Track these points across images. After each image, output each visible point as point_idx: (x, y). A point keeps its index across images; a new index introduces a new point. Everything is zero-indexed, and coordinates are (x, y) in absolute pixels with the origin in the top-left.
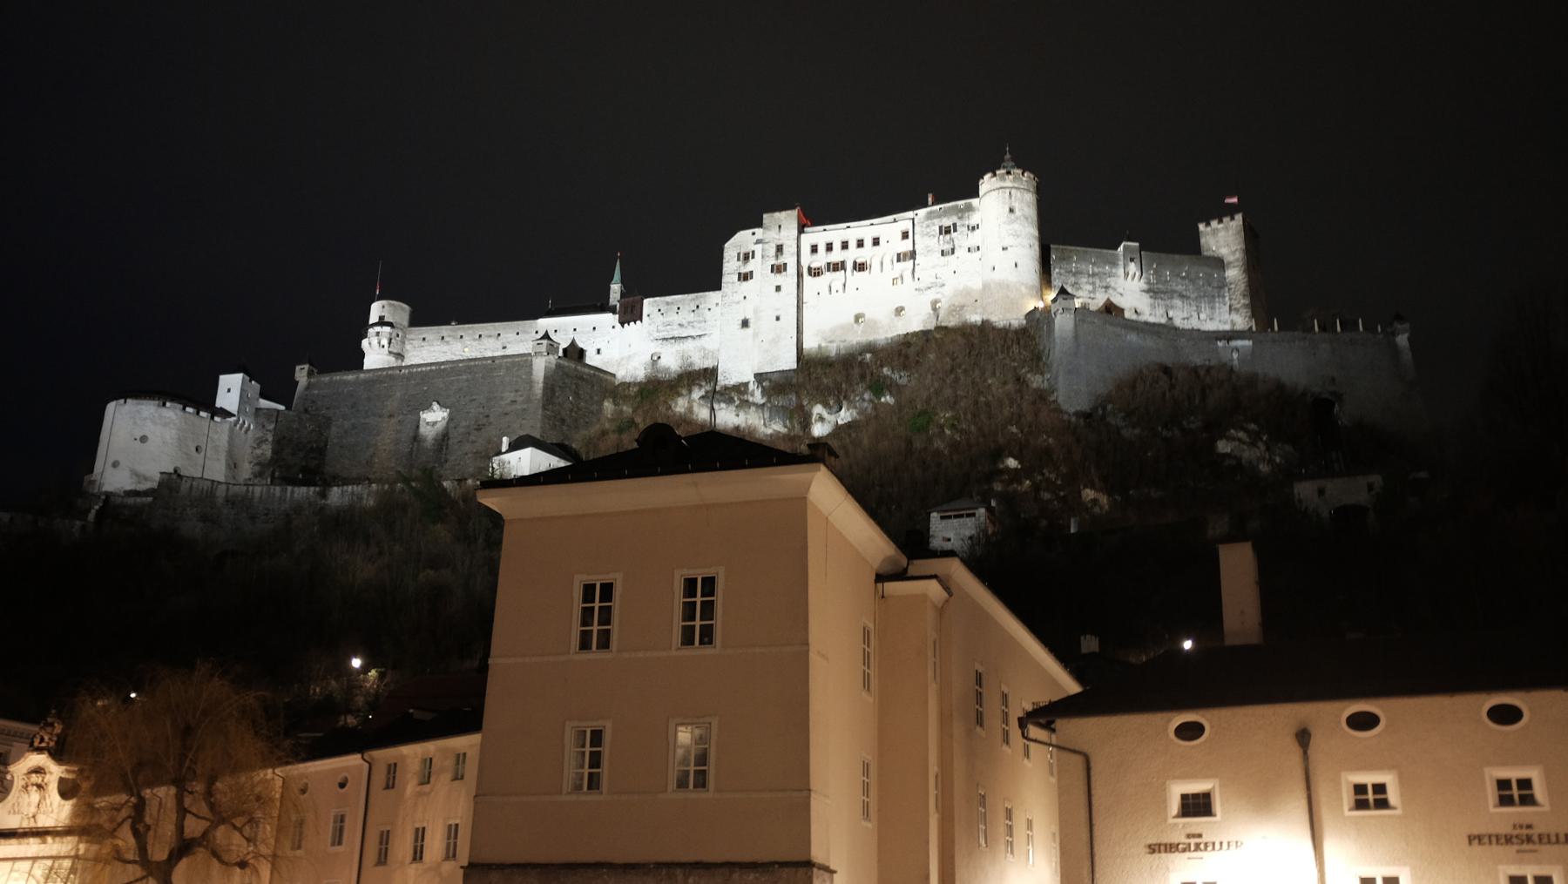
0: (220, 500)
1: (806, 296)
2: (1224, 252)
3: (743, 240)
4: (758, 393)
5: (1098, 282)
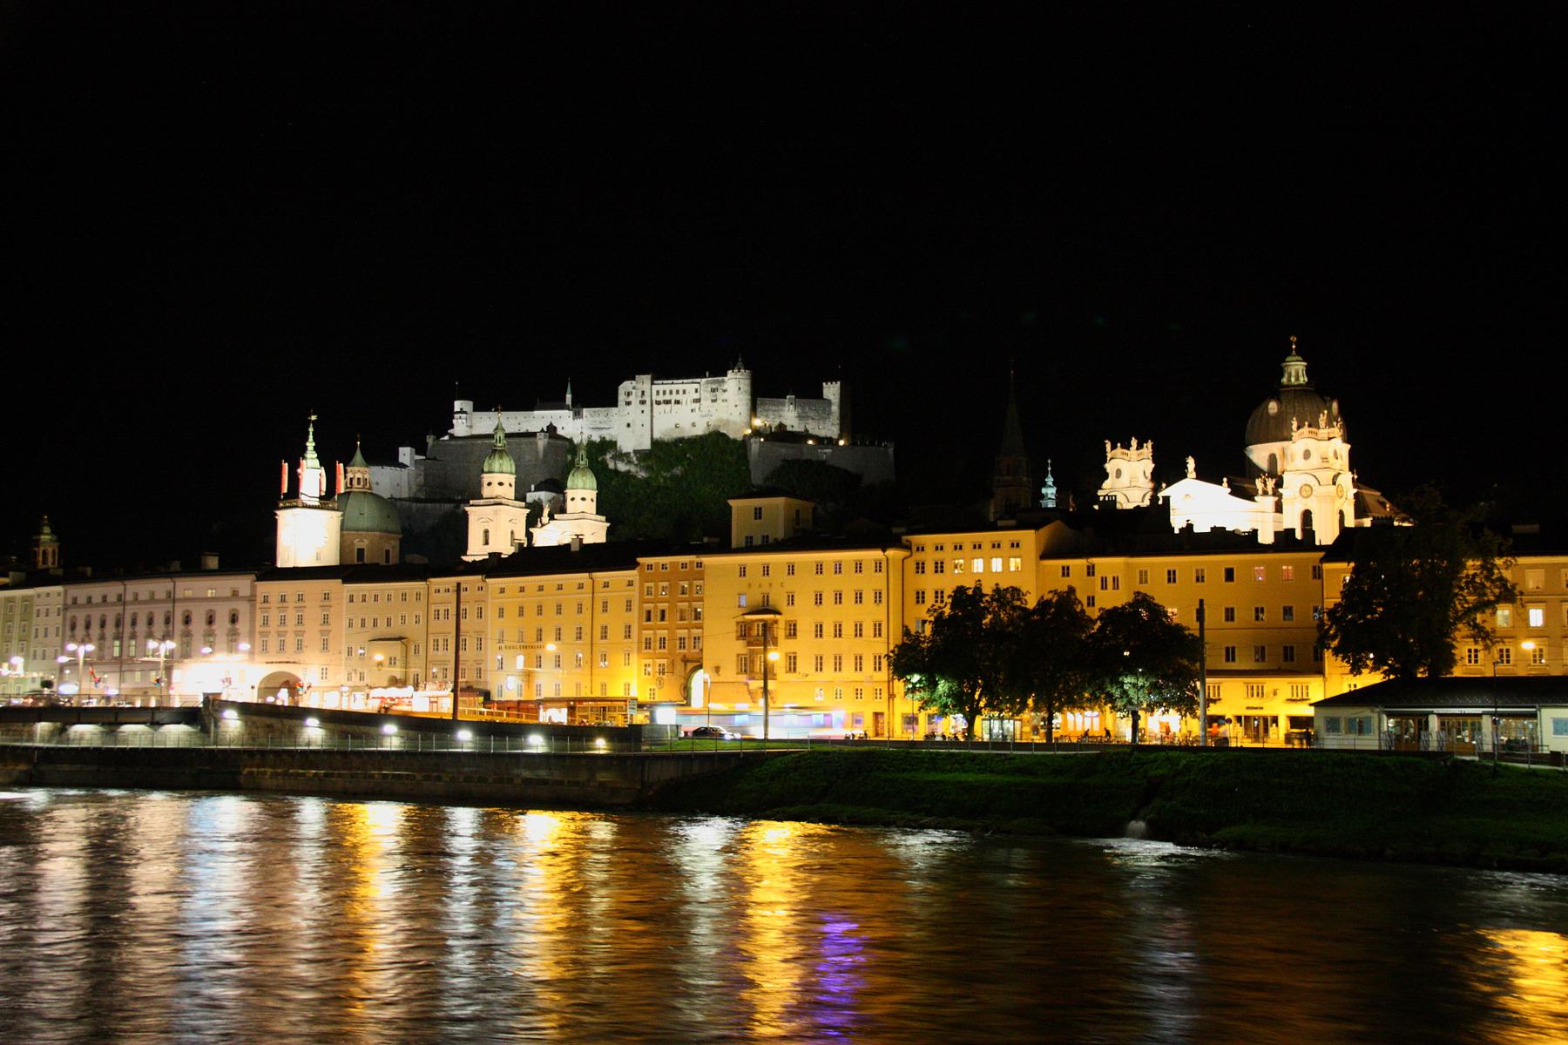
0: (414, 510)
1: (654, 415)
2: (831, 397)
3: (626, 386)
4: (634, 459)
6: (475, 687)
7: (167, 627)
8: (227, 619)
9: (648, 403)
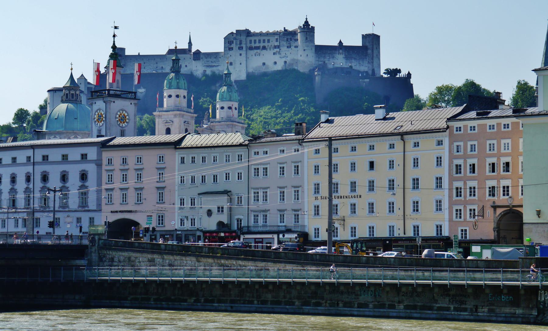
4: (235, 86)
5: (331, 56)
6: (293, 229)
7: (28, 185)
8: (78, 176)
9: (244, 49)
